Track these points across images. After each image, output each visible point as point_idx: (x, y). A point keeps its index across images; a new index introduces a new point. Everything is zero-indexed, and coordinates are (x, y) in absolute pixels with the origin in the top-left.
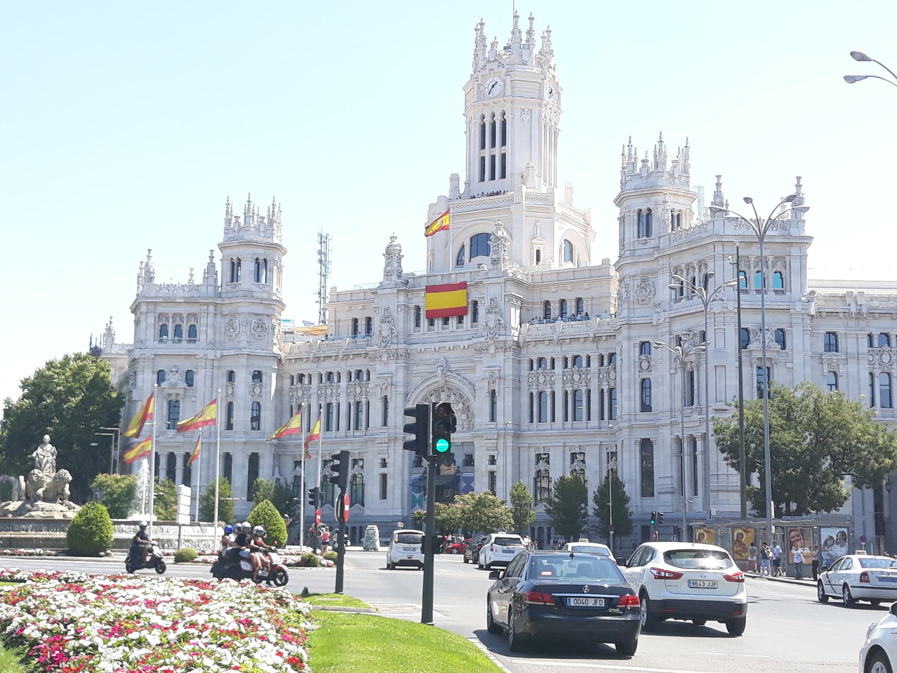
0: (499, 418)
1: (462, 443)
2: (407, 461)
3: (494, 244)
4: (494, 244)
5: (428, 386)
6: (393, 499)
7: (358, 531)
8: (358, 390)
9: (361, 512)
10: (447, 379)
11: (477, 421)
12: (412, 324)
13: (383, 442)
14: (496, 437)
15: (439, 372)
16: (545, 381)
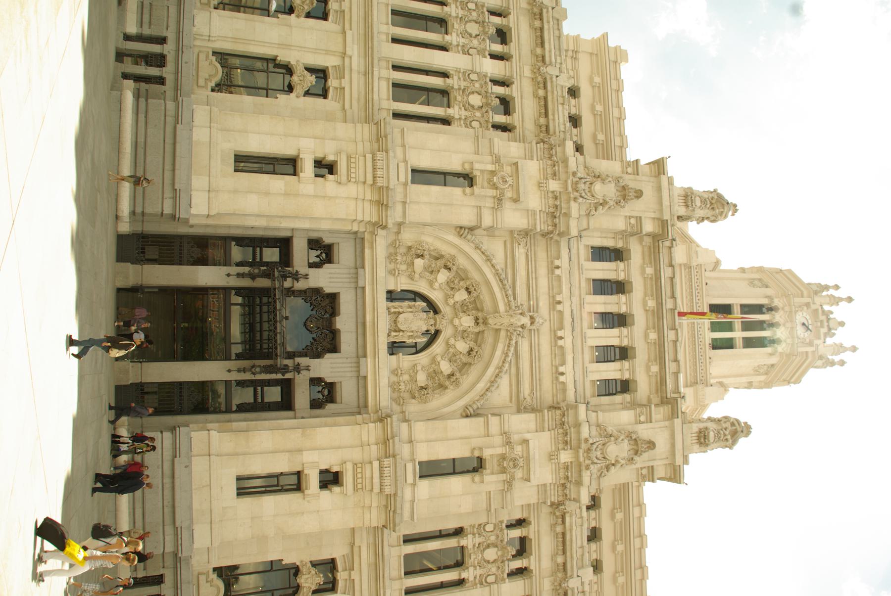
0: (425, 485)
1: (365, 378)
2: (325, 226)
3: (727, 433)
4: (727, 433)
5: (487, 283)
6: (235, 191)
7: (153, 71)
8: (476, 100)
9: (201, 82)
10: (503, 334)
11: (420, 429)
12: (598, 242)
13: (379, 173)
14: (388, 490)
15: (526, 320)
16: (488, 562)
